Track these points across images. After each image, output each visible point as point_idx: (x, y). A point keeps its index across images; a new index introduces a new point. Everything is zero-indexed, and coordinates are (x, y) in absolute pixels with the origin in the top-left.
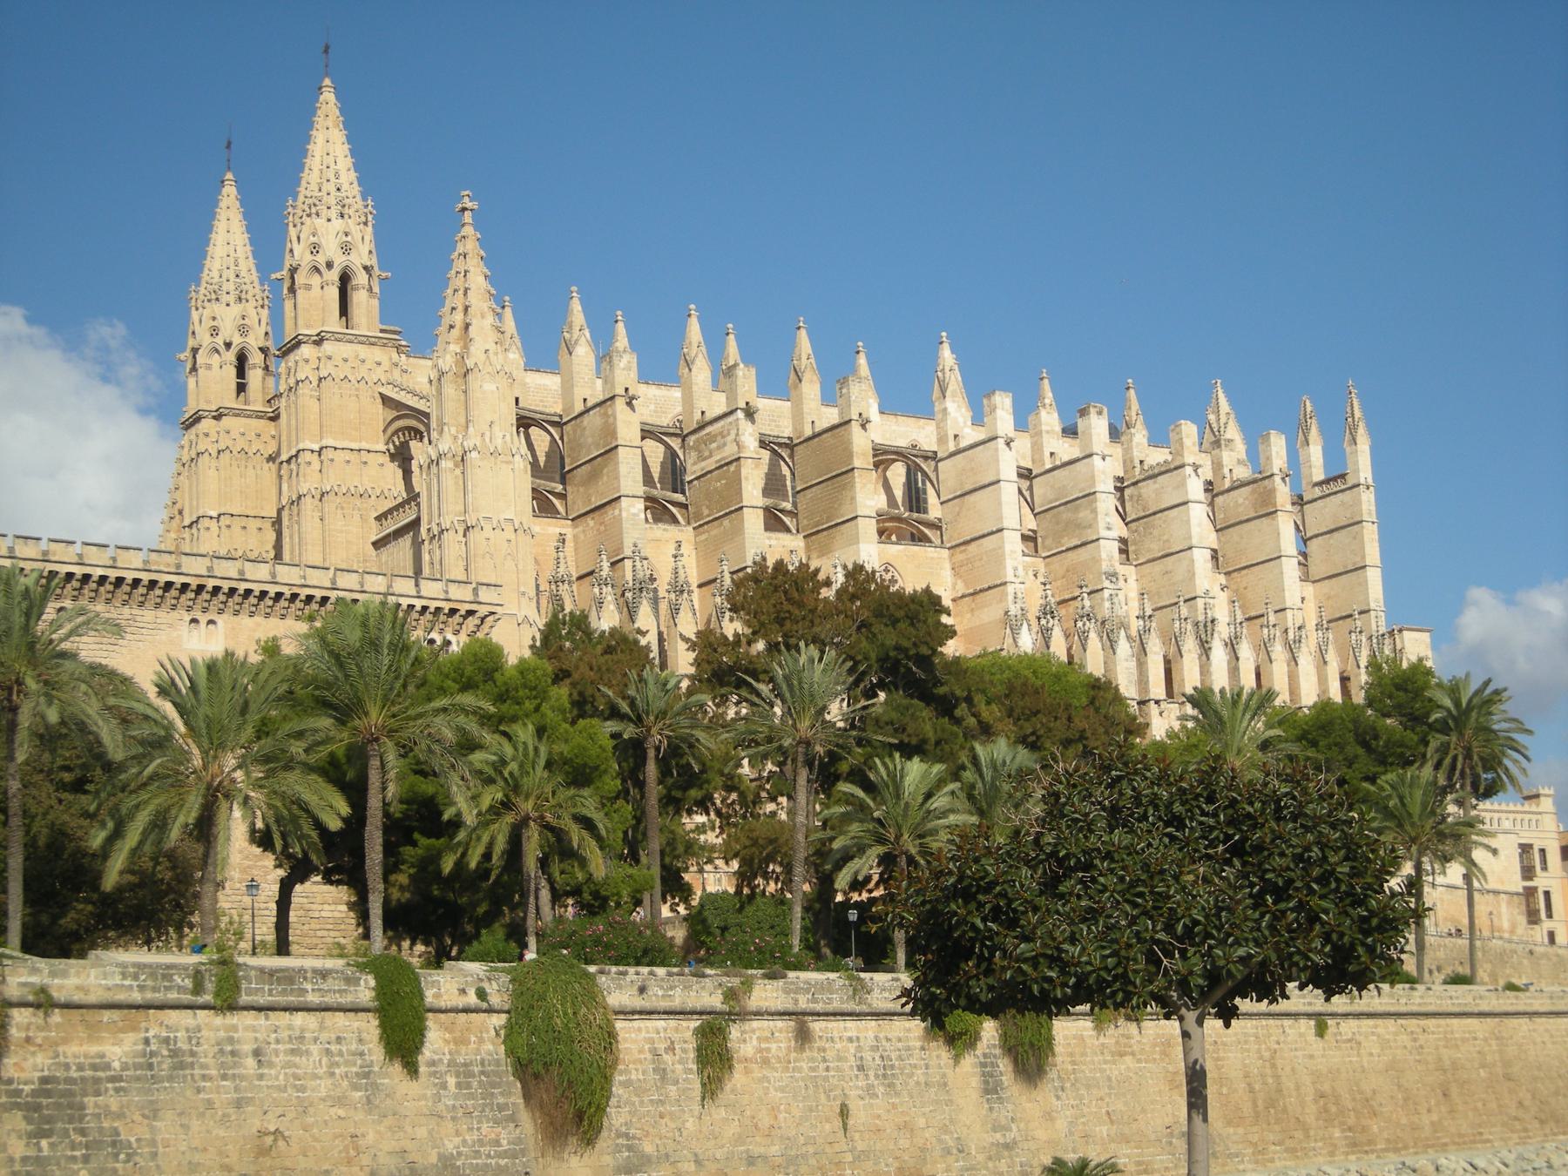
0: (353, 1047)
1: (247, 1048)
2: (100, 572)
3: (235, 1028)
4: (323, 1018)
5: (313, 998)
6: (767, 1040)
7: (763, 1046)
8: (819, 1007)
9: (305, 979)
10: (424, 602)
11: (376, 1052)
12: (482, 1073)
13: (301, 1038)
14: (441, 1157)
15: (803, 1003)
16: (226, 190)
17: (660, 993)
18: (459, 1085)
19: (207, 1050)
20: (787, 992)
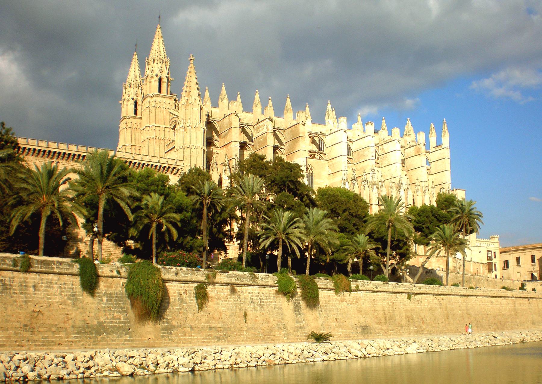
0: (70, 286)
1: (31, 285)
2: (64, 151)
3: (27, 278)
4: (60, 277)
5: (57, 270)
6: (220, 291)
7: (218, 293)
8: (239, 282)
9: (54, 264)
10: (161, 164)
11: (78, 288)
12: (116, 297)
13: (51, 283)
14: (98, 322)
15: (234, 281)
16: (134, 57)
17: (183, 275)
18: (107, 300)
19: (16, 285)
20: (228, 277)
